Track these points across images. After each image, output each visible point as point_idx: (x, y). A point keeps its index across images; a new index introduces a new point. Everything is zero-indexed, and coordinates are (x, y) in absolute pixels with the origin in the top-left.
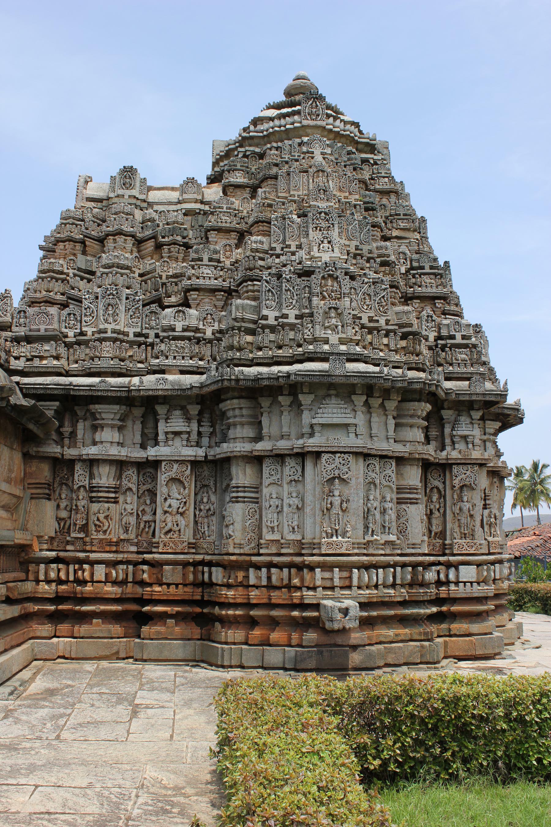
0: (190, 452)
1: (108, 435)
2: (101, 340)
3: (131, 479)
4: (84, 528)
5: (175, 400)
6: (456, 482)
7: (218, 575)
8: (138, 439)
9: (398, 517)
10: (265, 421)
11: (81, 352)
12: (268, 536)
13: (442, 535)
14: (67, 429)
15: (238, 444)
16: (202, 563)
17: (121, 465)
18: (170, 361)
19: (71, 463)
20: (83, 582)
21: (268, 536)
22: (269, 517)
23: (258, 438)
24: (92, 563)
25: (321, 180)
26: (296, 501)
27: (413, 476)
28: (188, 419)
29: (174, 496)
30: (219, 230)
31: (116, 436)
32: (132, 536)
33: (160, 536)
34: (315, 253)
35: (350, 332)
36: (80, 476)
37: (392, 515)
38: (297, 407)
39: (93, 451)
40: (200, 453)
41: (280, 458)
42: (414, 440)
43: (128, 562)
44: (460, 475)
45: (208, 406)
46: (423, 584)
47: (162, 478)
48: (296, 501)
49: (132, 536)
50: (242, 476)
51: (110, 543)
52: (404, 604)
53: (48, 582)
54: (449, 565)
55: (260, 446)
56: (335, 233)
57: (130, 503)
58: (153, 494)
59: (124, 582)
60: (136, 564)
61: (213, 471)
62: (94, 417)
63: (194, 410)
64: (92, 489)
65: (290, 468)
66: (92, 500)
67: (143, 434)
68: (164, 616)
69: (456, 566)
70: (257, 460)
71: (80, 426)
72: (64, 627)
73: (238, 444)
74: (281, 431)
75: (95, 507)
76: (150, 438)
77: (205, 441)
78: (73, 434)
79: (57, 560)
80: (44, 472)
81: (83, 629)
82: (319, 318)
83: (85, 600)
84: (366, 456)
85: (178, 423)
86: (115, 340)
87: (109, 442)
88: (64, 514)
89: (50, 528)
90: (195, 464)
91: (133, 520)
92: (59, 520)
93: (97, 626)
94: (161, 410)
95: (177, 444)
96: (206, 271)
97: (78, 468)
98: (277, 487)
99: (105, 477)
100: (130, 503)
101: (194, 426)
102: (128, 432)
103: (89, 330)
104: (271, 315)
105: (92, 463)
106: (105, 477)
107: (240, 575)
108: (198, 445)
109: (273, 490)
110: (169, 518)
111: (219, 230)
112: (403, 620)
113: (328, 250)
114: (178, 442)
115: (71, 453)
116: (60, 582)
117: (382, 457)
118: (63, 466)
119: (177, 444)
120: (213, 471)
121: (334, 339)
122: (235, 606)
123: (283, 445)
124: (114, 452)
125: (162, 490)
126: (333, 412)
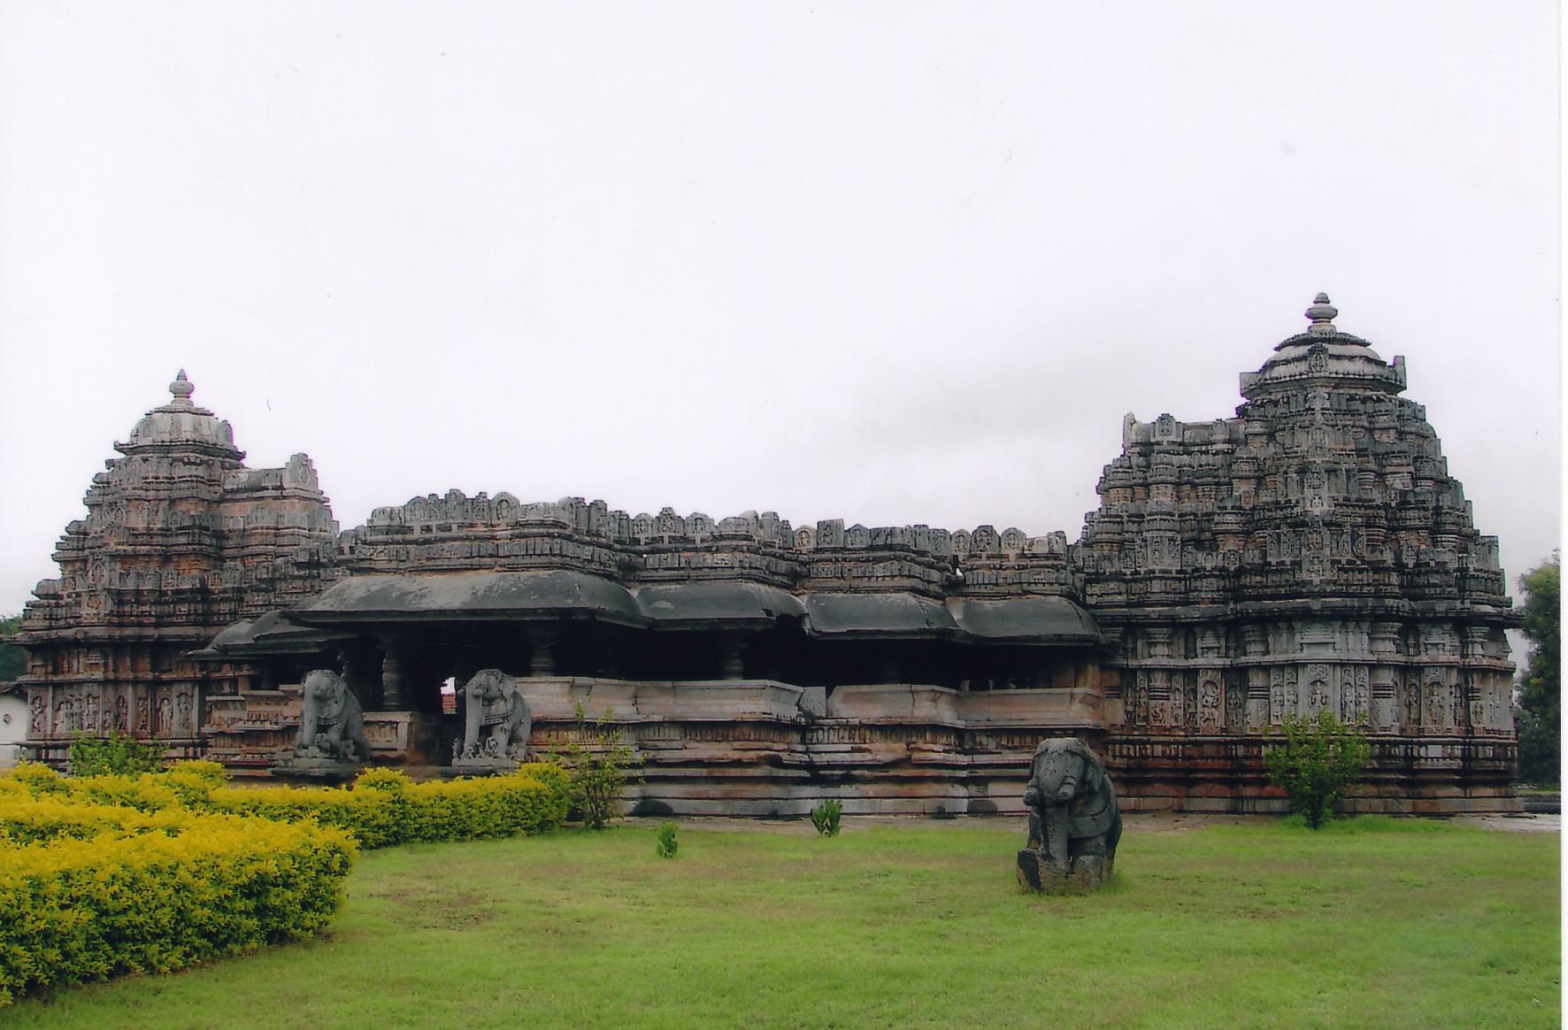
0: (1219, 662)
1: (1160, 650)
2: (1150, 579)
3: (1178, 682)
4: (1146, 719)
5: (1210, 624)
6: (1428, 680)
8: (1183, 652)
9: (1371, 709)
10: (1270, 639)
11: (1136, 587)
12: (1274, 722)
13: (1418, 721)
14: (1130, 645)
16: (1232, 742)
17: (1170, 672)
18: (1203, 595)
19: (1133, 672)
20: (1146, 757)
21: (1274, 722)
22: (1276, 709)
23: (1267, 652)
24: (1153, 744)
25: (1318, 436)
26: (1293, 698)
27: (1386, 678)
28: (1218, 637)
29: (1209, 695)
30: (1241, 478)
31: (1166, 651)
32: (1181, 723)
33: (1200, 724)
34: (1308, 508)
35: (1328, 576)
36: (1141, 681)
37: (1365, 706)
38: (1291, 630)
39: (1149, 662)
40: (1228, 662)
41: (1281, 667)
42: (1387, 650)
43: (1178, 743)
44: (1430, 676)
46: (1390, 757)
47: (1201, 680)
48: (1293, 698)
49: (1181, 723)
50: (1256, 680)
51: (1165, 729)
52: (1374, 770)
53: (1122, 756)
54: (1421, 744)
55: (1267, 658)
56: (1324, 493)
57: (1179, 699)
58: (1195, 692)
59: (1176, 757)
60: (1183, 744)
61: (1236, 677)
62: (1149, 636)
63: (1222, 631)
64: (1150, 689)
66: (1150, 698)
67: (1186, 648)
68: (1204, 781)
69: (1425, 744)
70: (1265, 668)
71: (1139, 644)
72: (1134, 790)
73: (1253, 657)
74: (1282, 649)
75: (1153, 703)
76: (1190, 653)
77: (1232, 653)
78: (1135, 649)
79: (1128, 742)
80: (1115, 679)
81: (1148, 790)
82: (1305, 566)
83: (1148, 770)
84: (1343, 665)
85: (1210, 641)
86: (1161, 578)
87: (1161, 656)
88: (1130, 708)
89: (1120, 718)
90: (1224, 671)
91: (1181, 712)
92: (1127, 713)
93: (1158, 788)
94: (1198, 630)
95: (1209, 658)
96: (1230, 518)
97: (1140, 676)
98: (1281, 691)
99: (1159, 681)
100: (1179, 699)
101: (1223, 642)
102: (1175, 647)
103: (1142, 570)
104: (1273, 560)
105: (1149, 671)
107: (1256, 750)
108: (1227, 656)
109: (1277, 689)
110: (1206, 711)
111: (1241, 478)
112: (1375, 782)
114: (1211, 654)
115: (1133, 663)
116: (1129, 757)
117: (1356, 665)
118: (1129, 674)
120: (1236, 677)
121: (1316, 580)
122: (1252, 771)
123: (1281, 658)
124: (1165, 662)
125: (1201, 690)
126: (1316, 634)
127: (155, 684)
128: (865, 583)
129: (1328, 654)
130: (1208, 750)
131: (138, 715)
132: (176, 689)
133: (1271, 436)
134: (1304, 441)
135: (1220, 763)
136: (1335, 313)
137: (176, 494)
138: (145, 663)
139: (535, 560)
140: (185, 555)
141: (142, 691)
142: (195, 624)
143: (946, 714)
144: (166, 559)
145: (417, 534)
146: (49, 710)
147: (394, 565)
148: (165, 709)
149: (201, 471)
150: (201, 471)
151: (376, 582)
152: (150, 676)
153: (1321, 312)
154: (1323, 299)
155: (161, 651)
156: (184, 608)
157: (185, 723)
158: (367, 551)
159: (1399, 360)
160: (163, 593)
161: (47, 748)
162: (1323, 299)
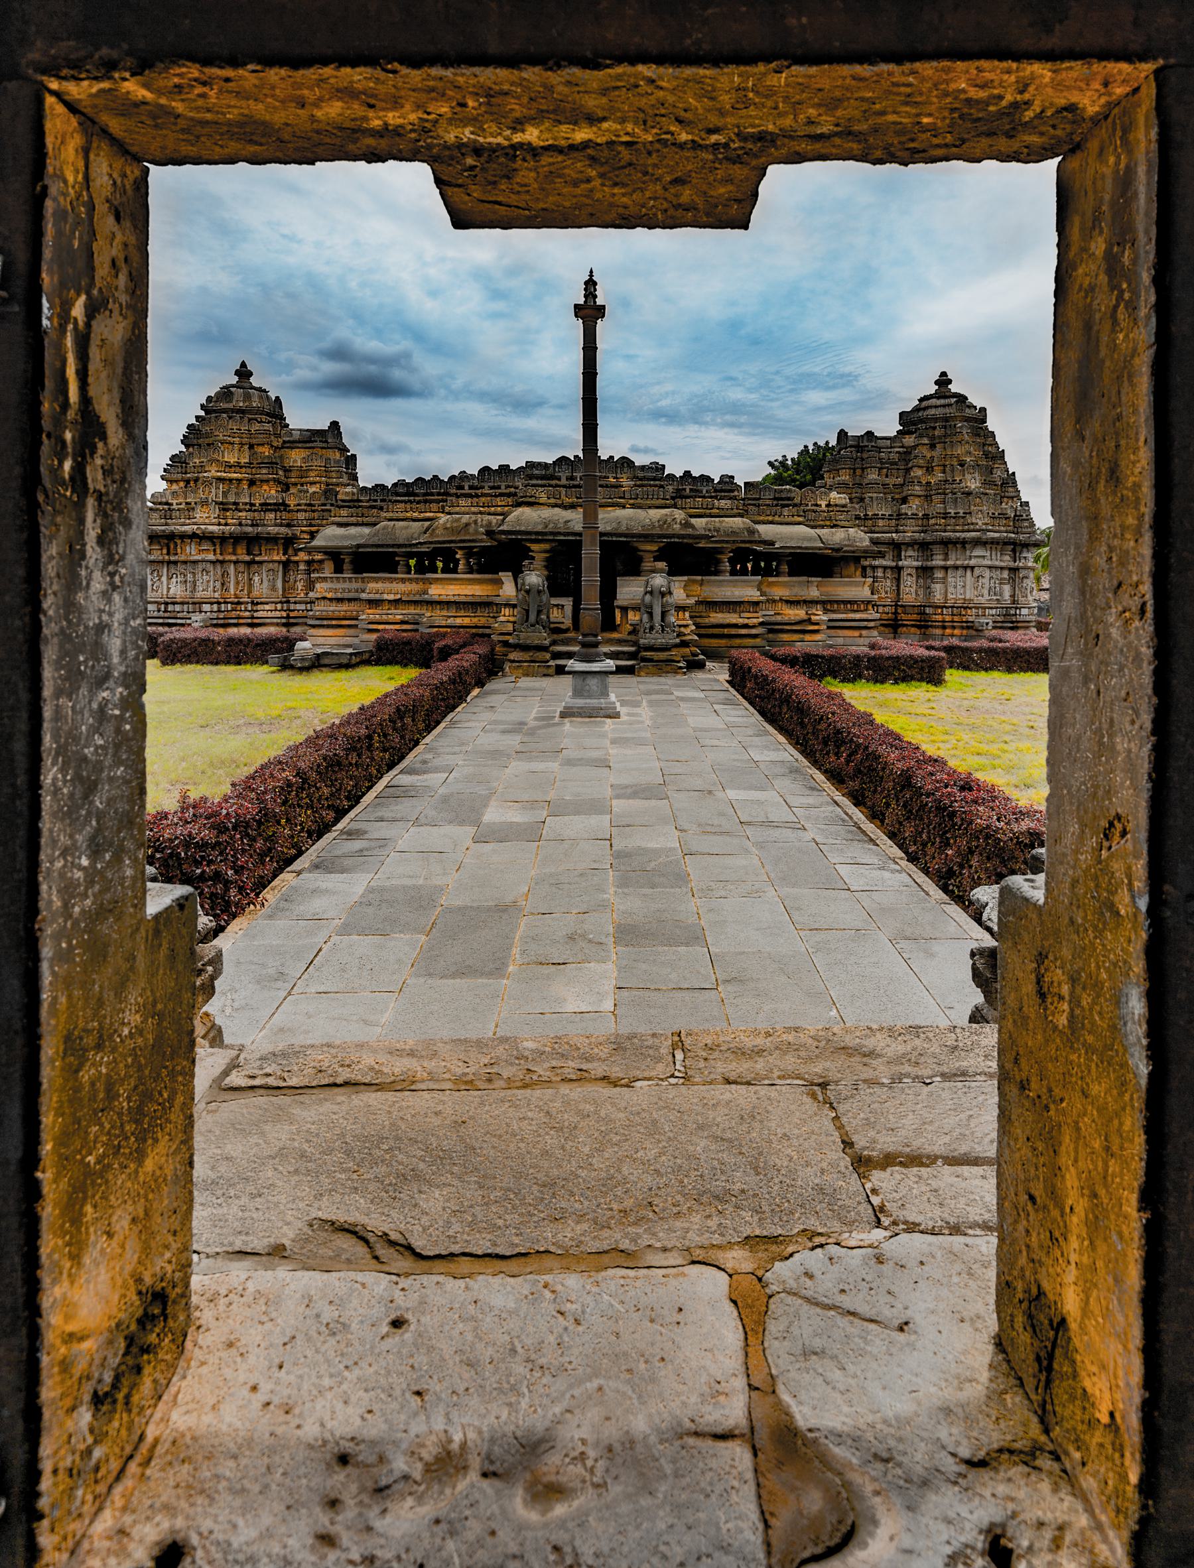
0: (915, 564)
5: (911, 544)
7: (928, 610)
15: (938, 561)
17: (885, 568)
45: (924, 547)
50: (939, 574)
61: (925, 572)
65: (960, 572)
70: (946, 568)
85: (910, 553)
95: (910, 561)
99: (880, 573)
106: (880, 573)
113: (973, 483)
119: (910, 561)
120: (925, 572)
127: (253, 562)
128: (777, 518)
129: (987, 562)
130: (910, 610)
131: (238, 583)
132: (264, 567)
133: (932, 447)
134: (959, 450)
135: (915, 617)
136: (950, 382)
137: (254, 441)
138: (242, 550)
139: (655, 502)
140: (267, 481)
141: (241, 568)
142: (281, 525)
143: (814, 593)
144: (252, 483)
145: (564, 482)
146: (164, 579)
147: (552, 501)
148: (256, 578)
149: (268, 427)
150: (268, 427)
151: (546, 513)
152: (247, 558)
153: (943, 381)
154: (944, 374)
155: (253, 542)
156: (272, 516)
157: (274, 588)
158: (531, 491)
159: (983, 410)
160: (252, 505)
161: (166, 604)
162: (944, 374)
